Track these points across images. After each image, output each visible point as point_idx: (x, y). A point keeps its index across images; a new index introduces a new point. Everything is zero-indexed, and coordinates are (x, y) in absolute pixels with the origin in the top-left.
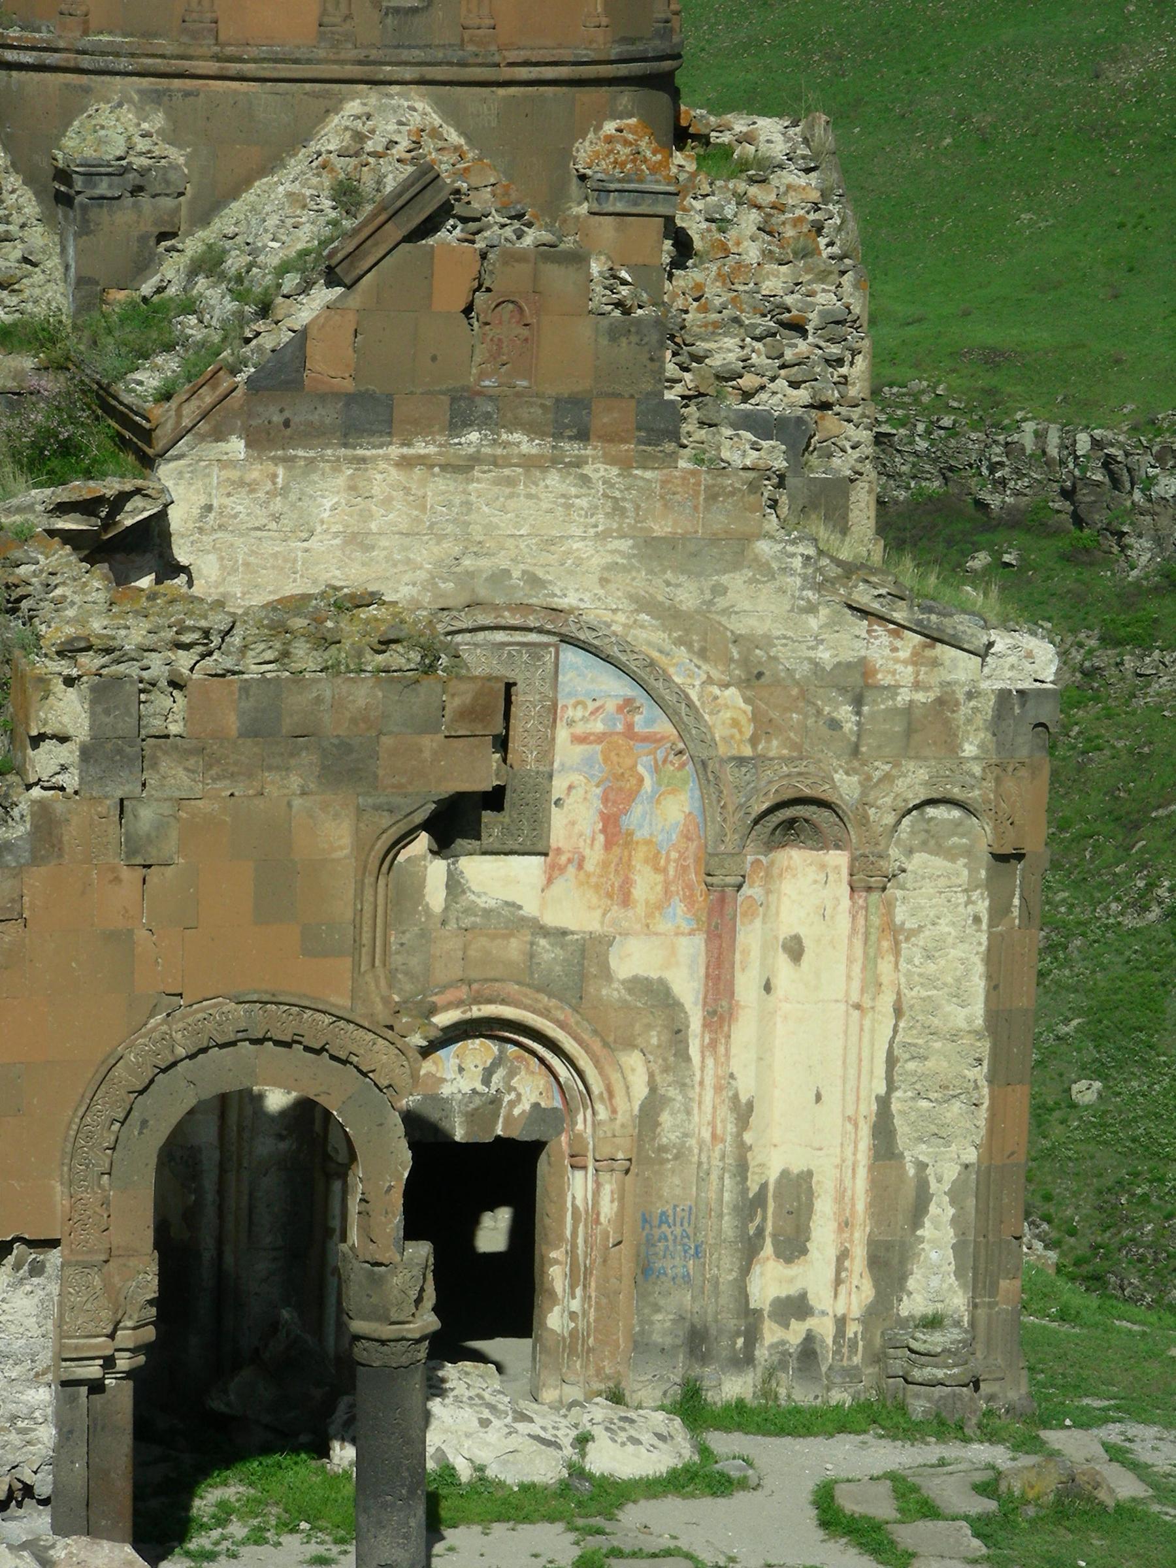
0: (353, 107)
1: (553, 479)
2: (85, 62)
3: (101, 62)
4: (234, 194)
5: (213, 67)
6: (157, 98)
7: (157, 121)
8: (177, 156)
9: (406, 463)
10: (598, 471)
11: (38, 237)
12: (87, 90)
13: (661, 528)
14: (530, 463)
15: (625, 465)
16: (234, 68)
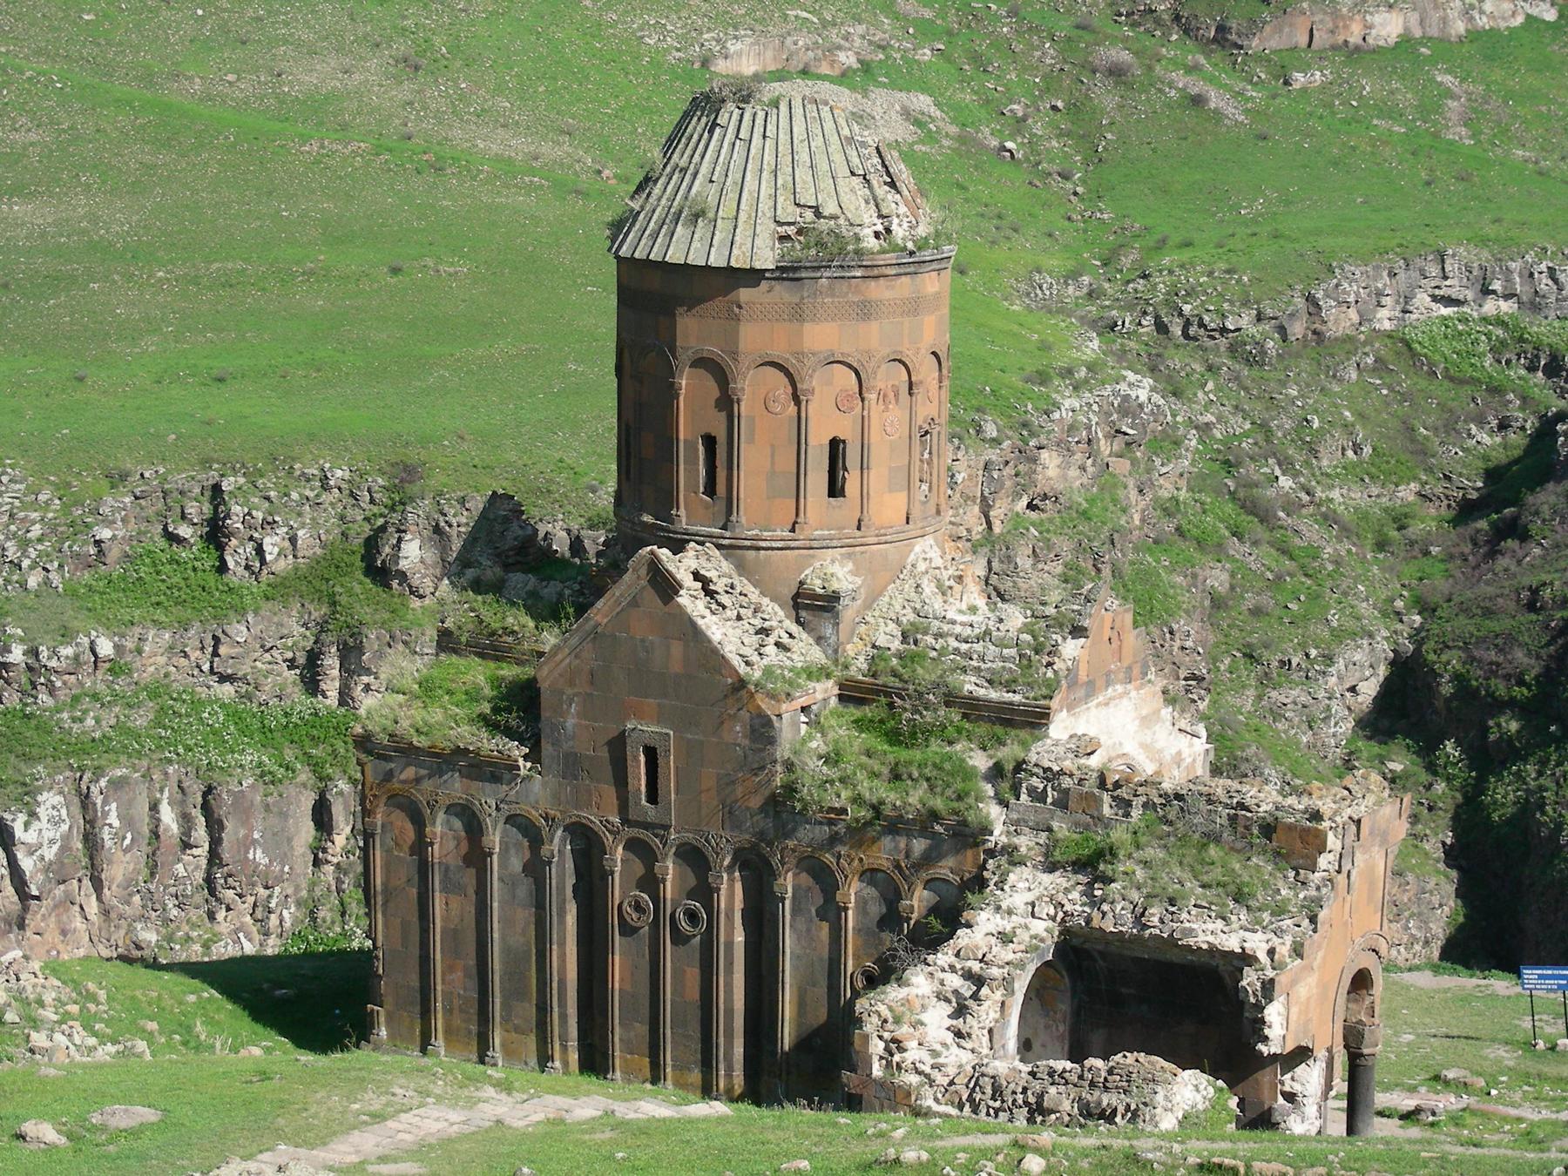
0: (917, 549)
1: (1125, 701)
2: (815, 544)
3: (825, 543)
4: (881, 594)
5: (876, 540)
6: (849, 556)
7: (850, 566)
8: (859, 581)
9: (1098, 705)
10: (1133, 694)
11: (794, 628)
12: (813, 556)
13: (1144, 712)
14: (1121, 696)
15: (1137, 689)
16: (883, 539)
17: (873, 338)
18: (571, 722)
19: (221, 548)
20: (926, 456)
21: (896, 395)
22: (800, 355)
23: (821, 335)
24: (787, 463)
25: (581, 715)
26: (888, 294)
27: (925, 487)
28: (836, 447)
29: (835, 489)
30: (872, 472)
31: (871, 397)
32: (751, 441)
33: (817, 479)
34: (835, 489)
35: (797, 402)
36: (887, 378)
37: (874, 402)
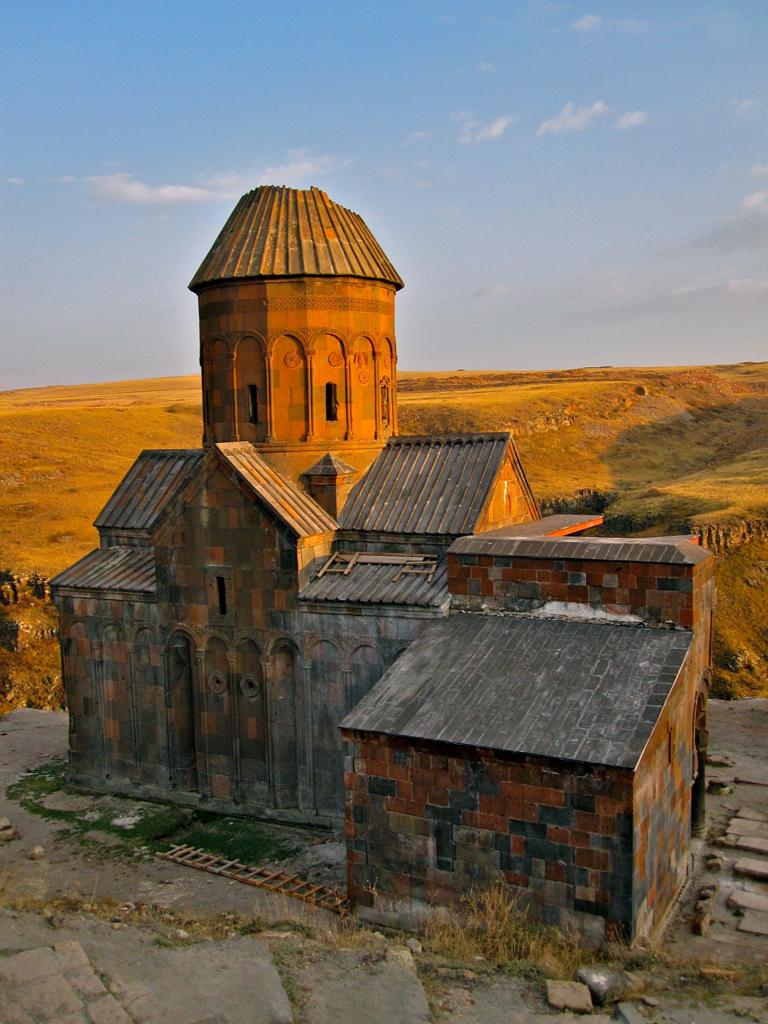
17: (350, 321)
18: (172, 567)
19: (60, 535)
20: (385, 402)
21: (366, 360)
22: (305, 330)
23: (316, 318)
24: (299, 398)
25: (179, 561)
26: (358, 296)
27: (386, 421)
28: (330, 389)
29: (331, 415)
30: (353, 405)
31: (351, 358)
32: (277, 385)
33: (319, 409)
34: (331, 415)
35: (305, 359)
36: (359, 347)
37: (352, 361)
